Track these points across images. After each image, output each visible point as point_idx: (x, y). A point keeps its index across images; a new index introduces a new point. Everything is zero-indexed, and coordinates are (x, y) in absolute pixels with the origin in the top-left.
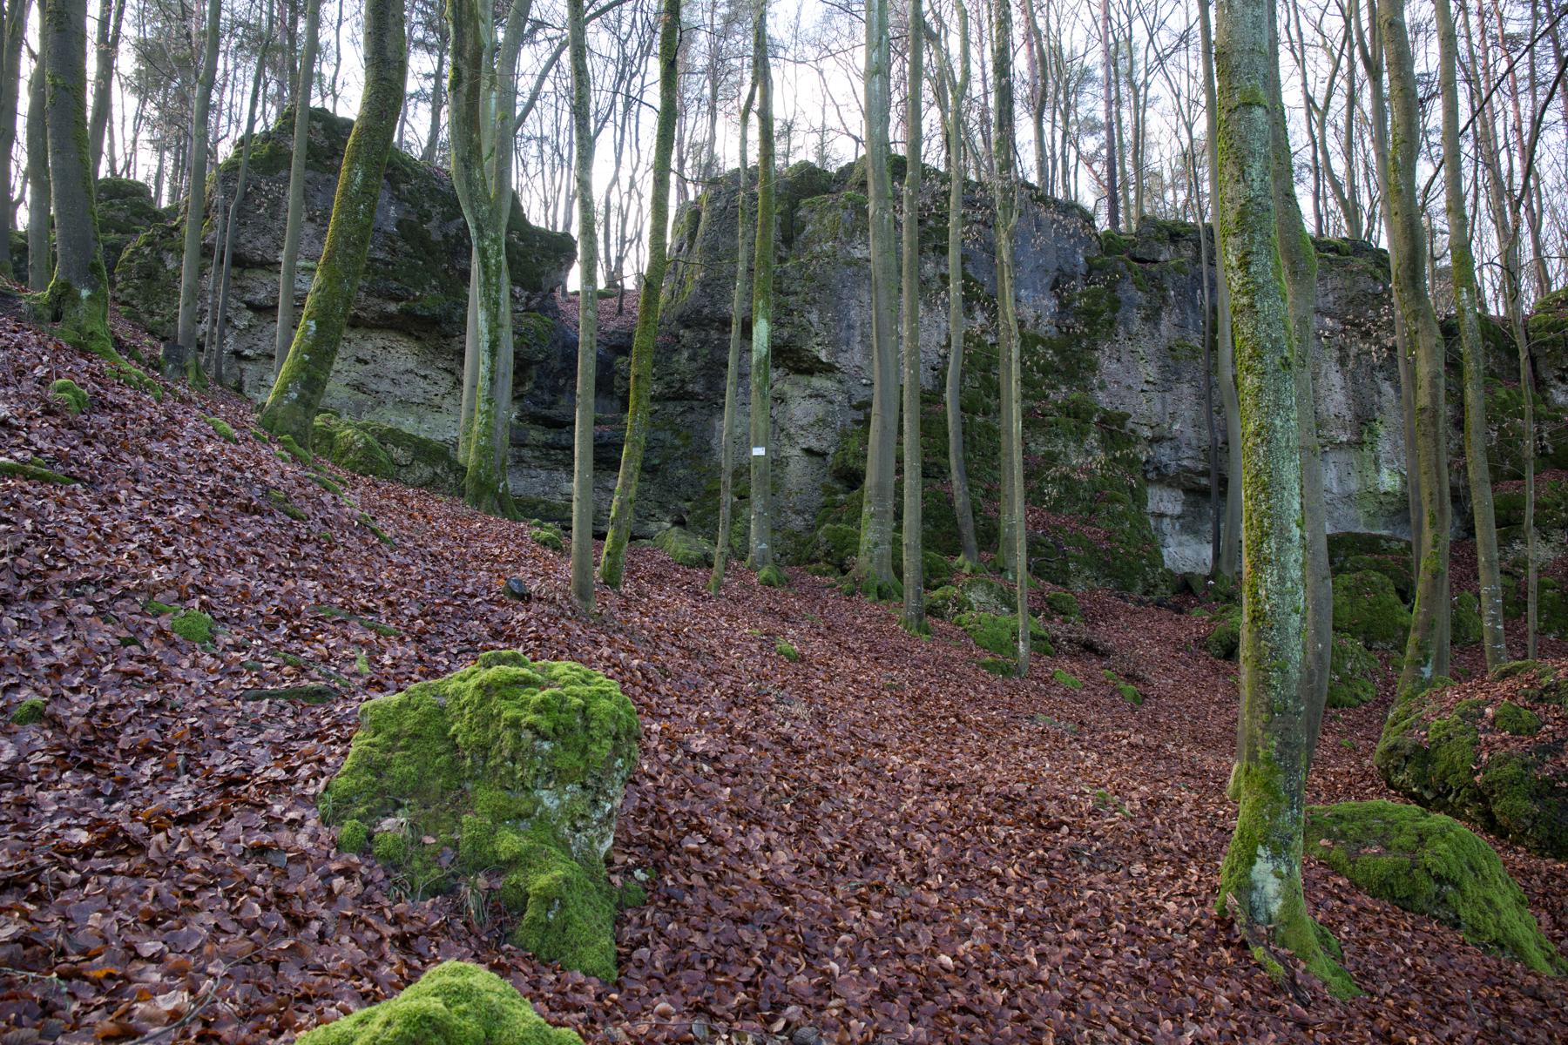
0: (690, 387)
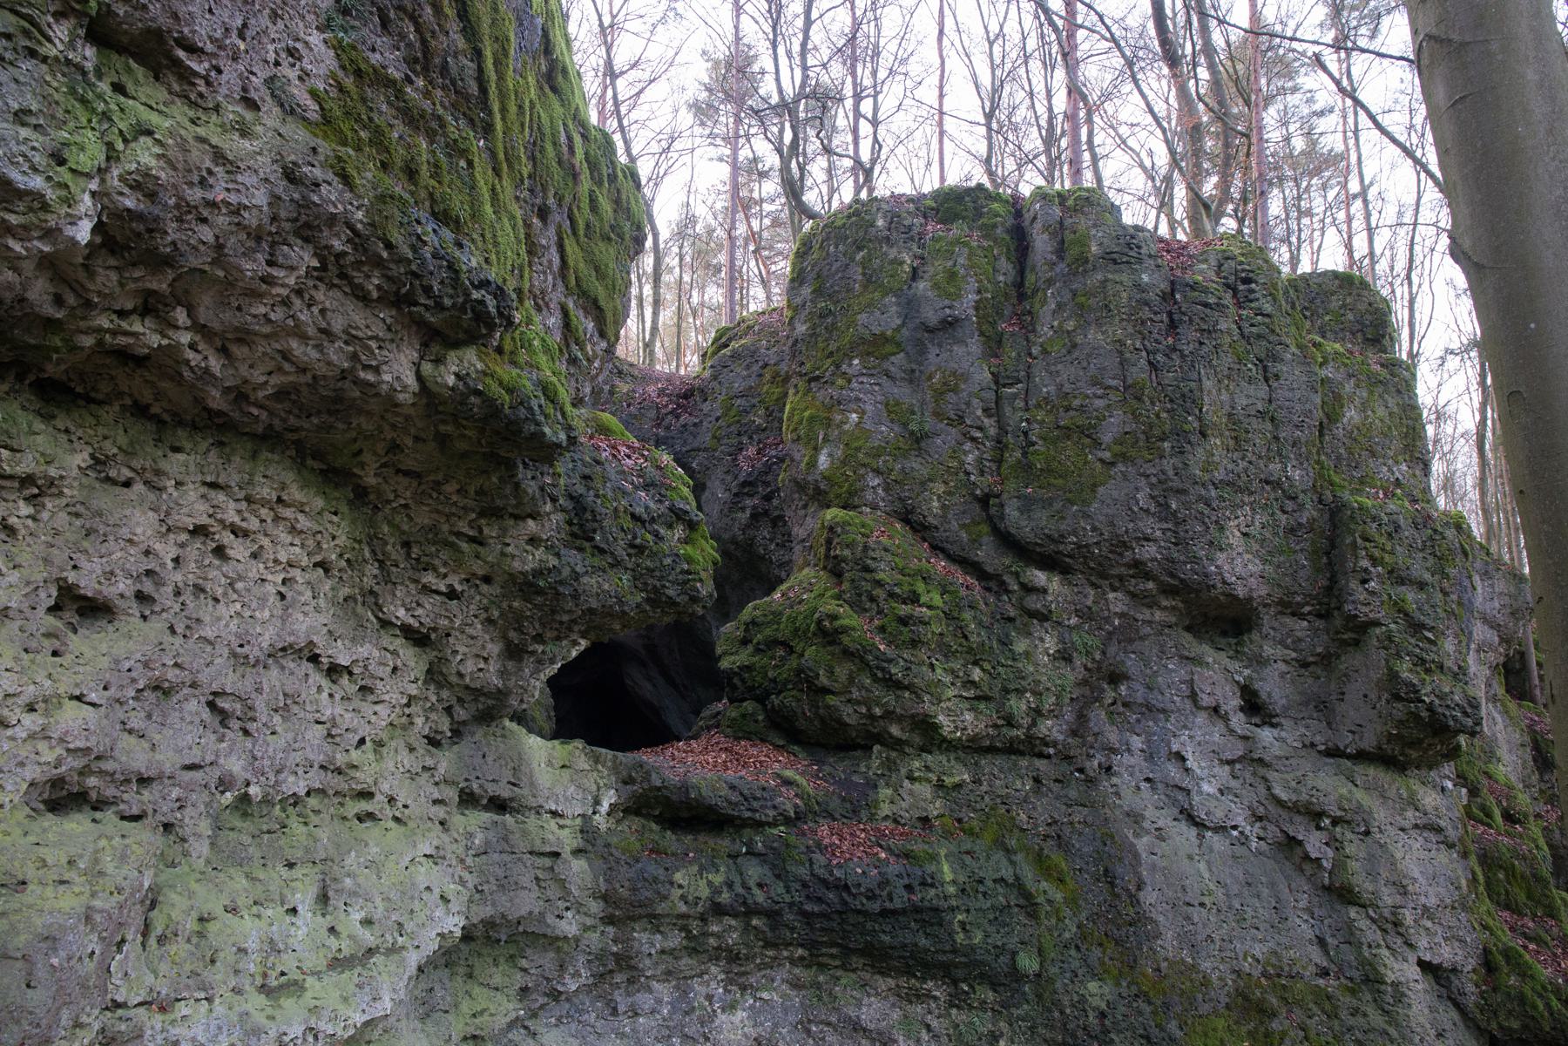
0: (1047, 727)
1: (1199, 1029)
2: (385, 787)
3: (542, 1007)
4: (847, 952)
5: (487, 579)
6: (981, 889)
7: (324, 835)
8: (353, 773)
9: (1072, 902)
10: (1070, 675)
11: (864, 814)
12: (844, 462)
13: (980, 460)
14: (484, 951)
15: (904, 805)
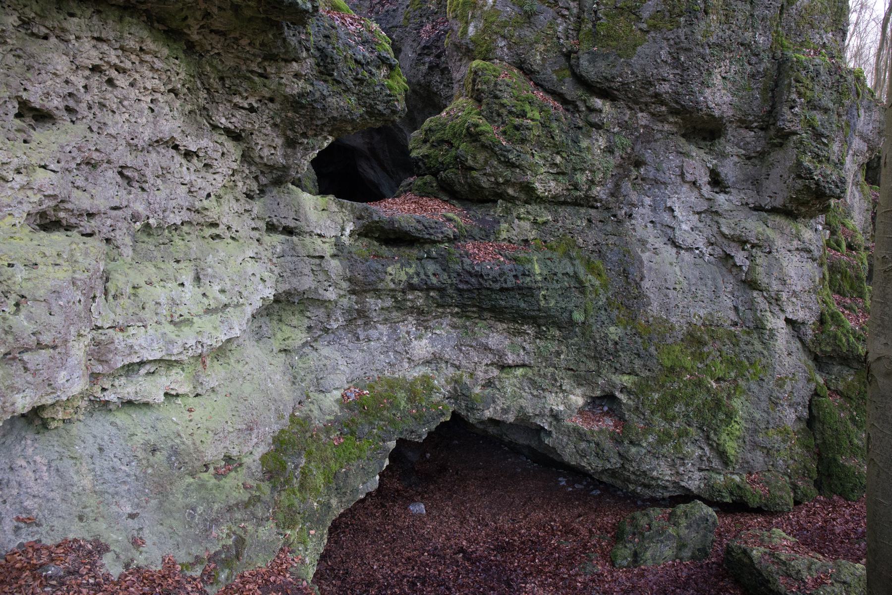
1: (666, 351)
2: (225, 220)
3: (319, 336)
4: (481, 309)
5: (272, 100)
6: (555, 278)
7: (193, 245)
8: (205, 213)
9: (604, 286)
10: (612, 161)
11: (492, 237)
12: (484, 32)
13: (566, 30)
14: (287, 308)
15: (514, 233)
